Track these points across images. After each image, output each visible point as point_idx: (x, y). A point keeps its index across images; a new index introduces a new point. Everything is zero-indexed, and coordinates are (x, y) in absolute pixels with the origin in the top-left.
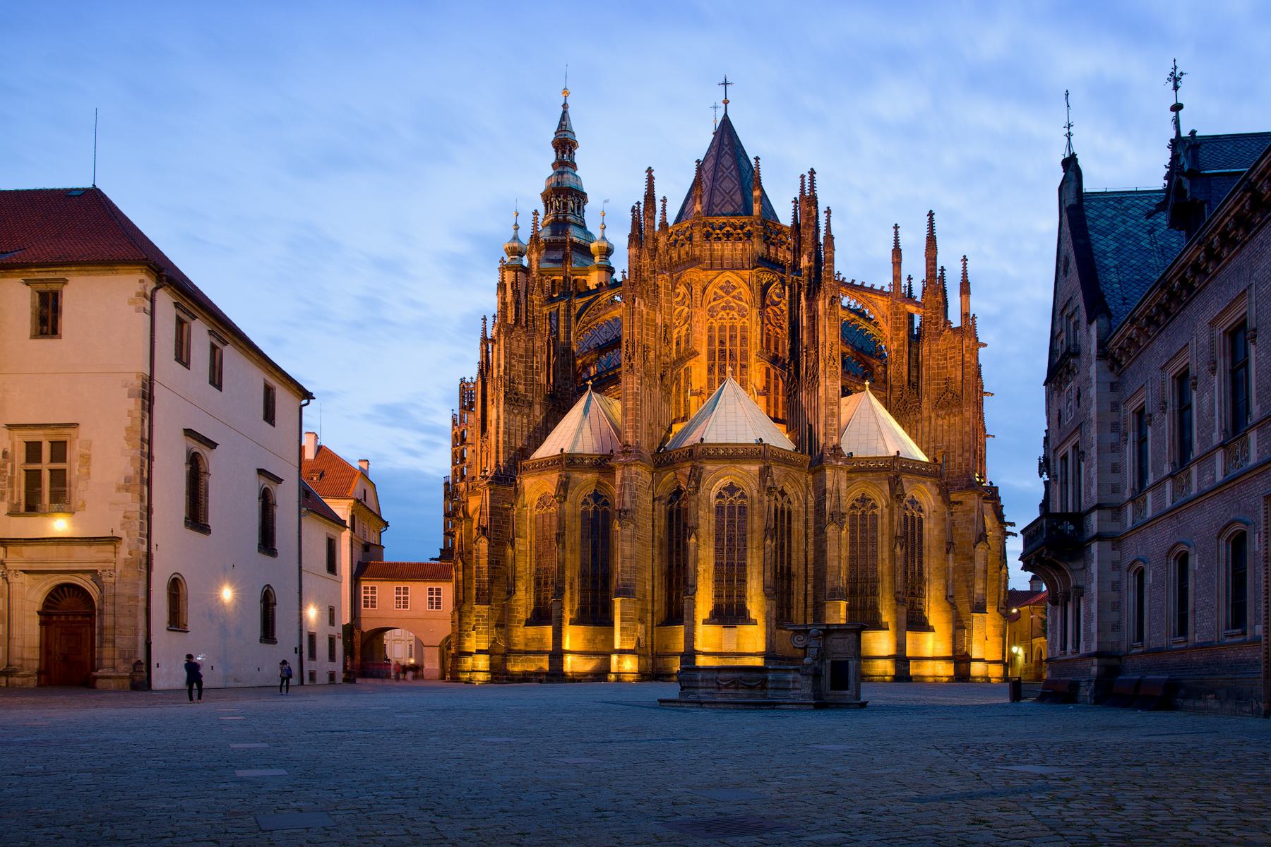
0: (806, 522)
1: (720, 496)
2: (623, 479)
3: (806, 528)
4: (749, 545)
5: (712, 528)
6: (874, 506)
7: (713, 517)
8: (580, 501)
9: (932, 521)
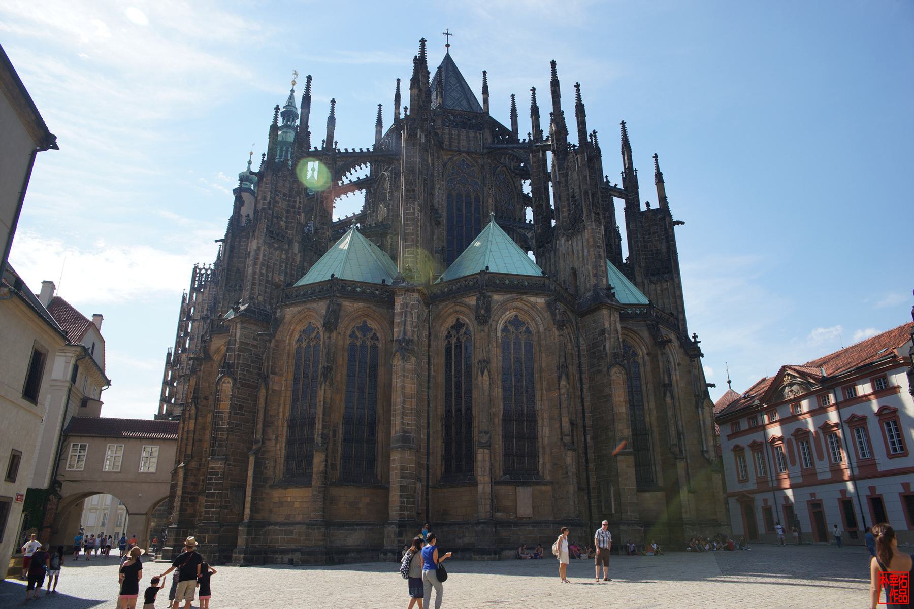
0: (580, 366)
1: (505, 329)
2: (403, 306)
3: (581, 372)
4: (537, 386)
5: (499, 365)
6: (635, 354)
7: (499, 351)
8: (349, 332)
9: (678, 373)
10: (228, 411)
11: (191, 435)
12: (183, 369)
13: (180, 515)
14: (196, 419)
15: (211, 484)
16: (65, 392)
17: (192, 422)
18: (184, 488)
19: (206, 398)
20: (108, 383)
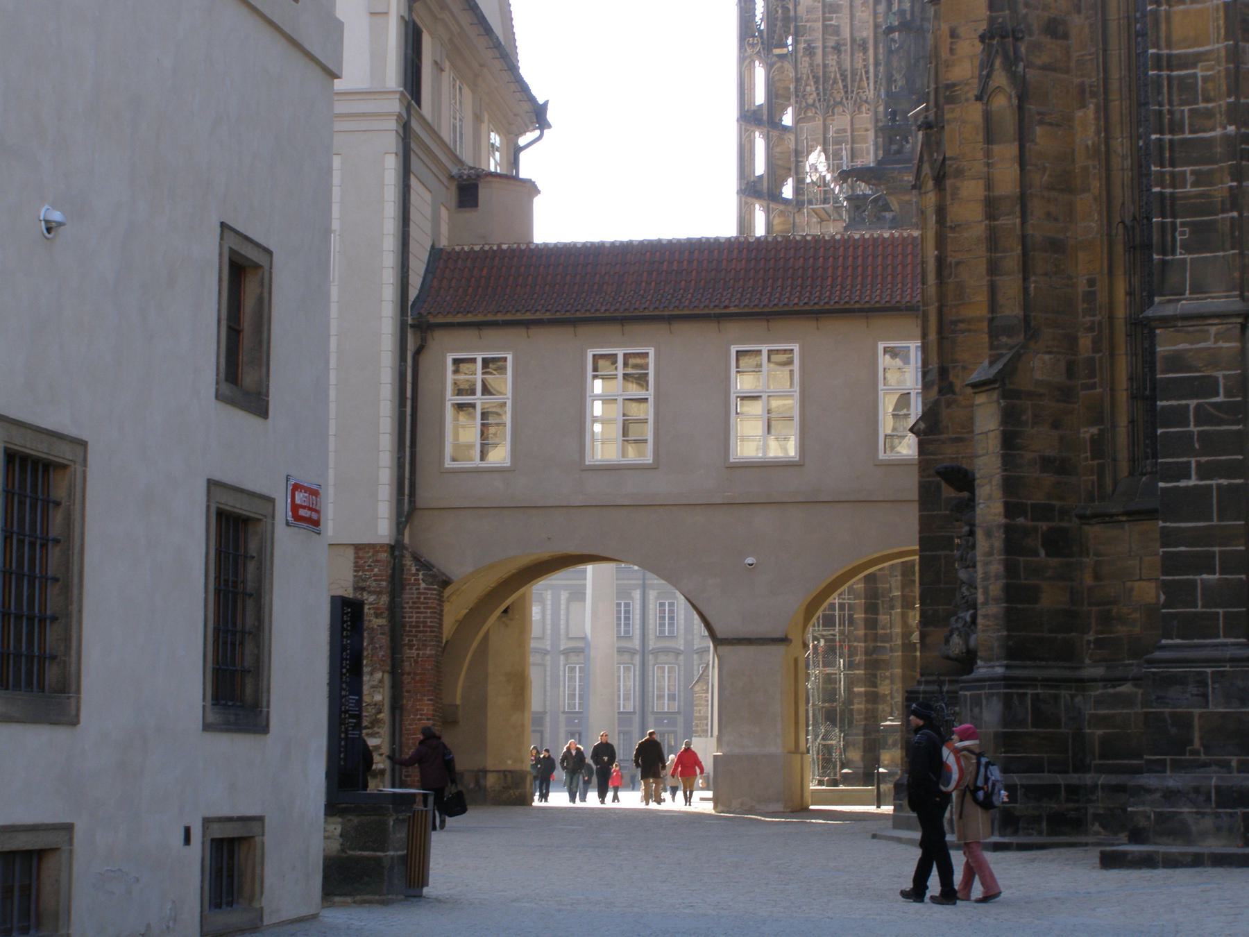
10: (1217, 46)
11: (1010, 221)
12: (810, 51)
13: (1012, 619)
14: (1023, 137)
15: (1183, 444)
16: (391, 141)
17: (1007, 151)
18: (1010, 485)
19: (1055, 29)
20: (538, 116)
